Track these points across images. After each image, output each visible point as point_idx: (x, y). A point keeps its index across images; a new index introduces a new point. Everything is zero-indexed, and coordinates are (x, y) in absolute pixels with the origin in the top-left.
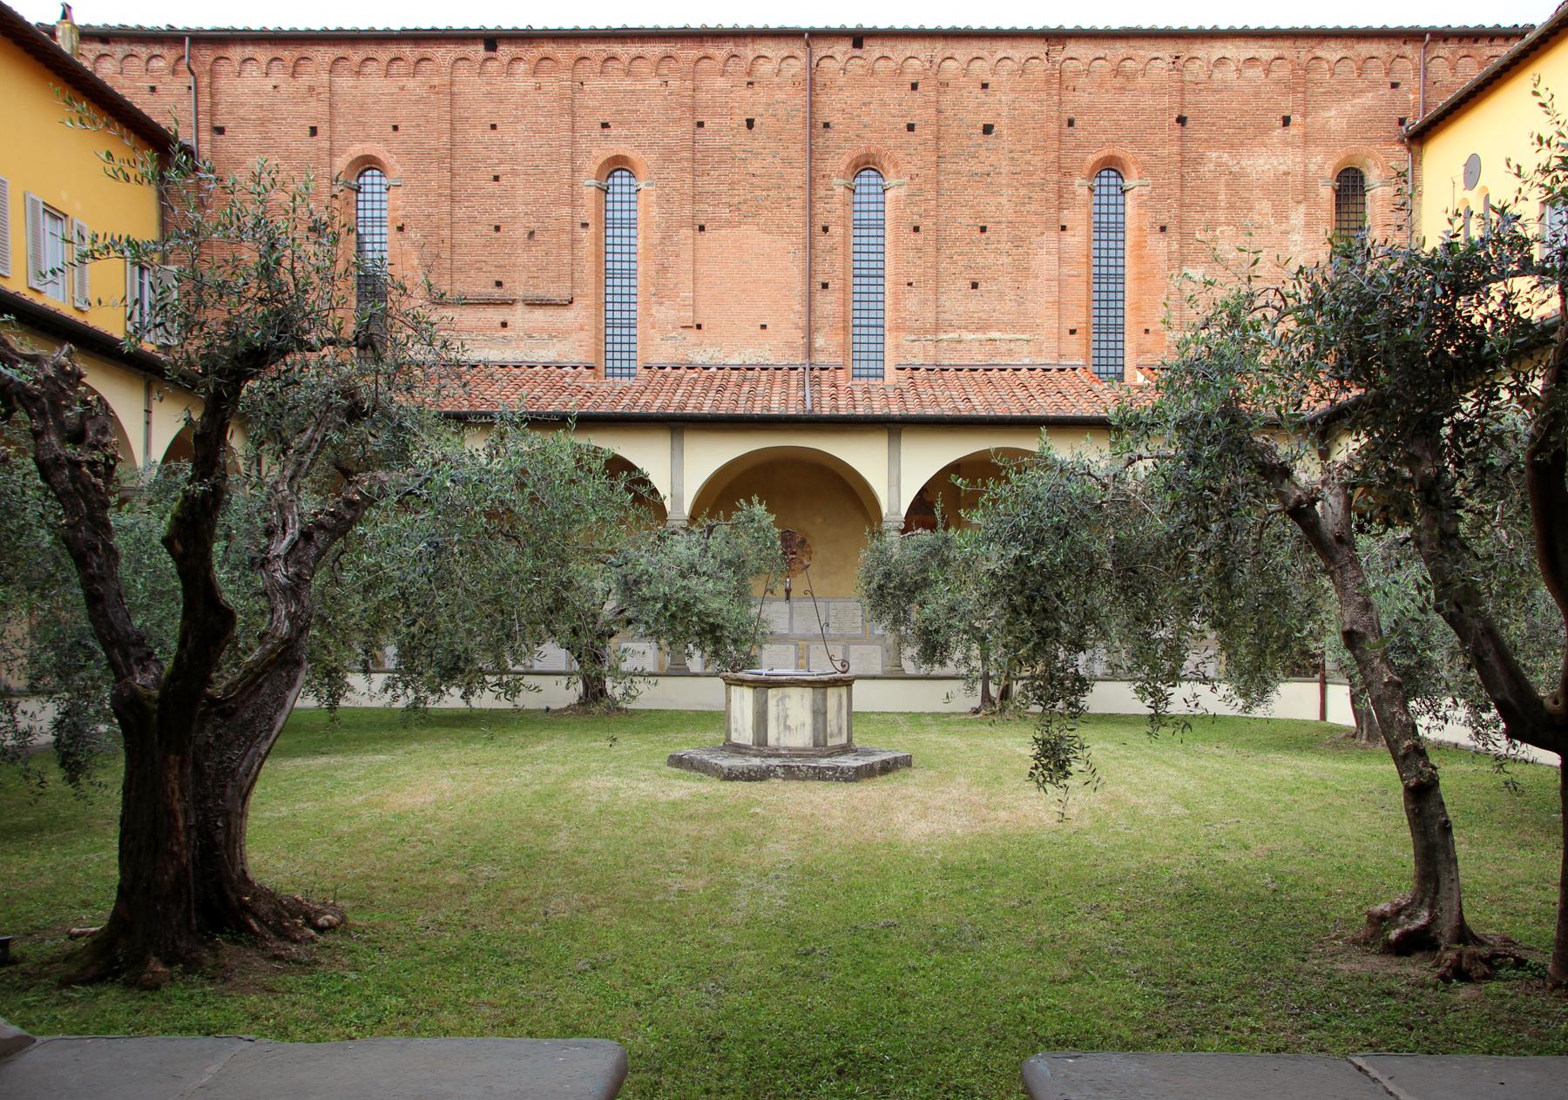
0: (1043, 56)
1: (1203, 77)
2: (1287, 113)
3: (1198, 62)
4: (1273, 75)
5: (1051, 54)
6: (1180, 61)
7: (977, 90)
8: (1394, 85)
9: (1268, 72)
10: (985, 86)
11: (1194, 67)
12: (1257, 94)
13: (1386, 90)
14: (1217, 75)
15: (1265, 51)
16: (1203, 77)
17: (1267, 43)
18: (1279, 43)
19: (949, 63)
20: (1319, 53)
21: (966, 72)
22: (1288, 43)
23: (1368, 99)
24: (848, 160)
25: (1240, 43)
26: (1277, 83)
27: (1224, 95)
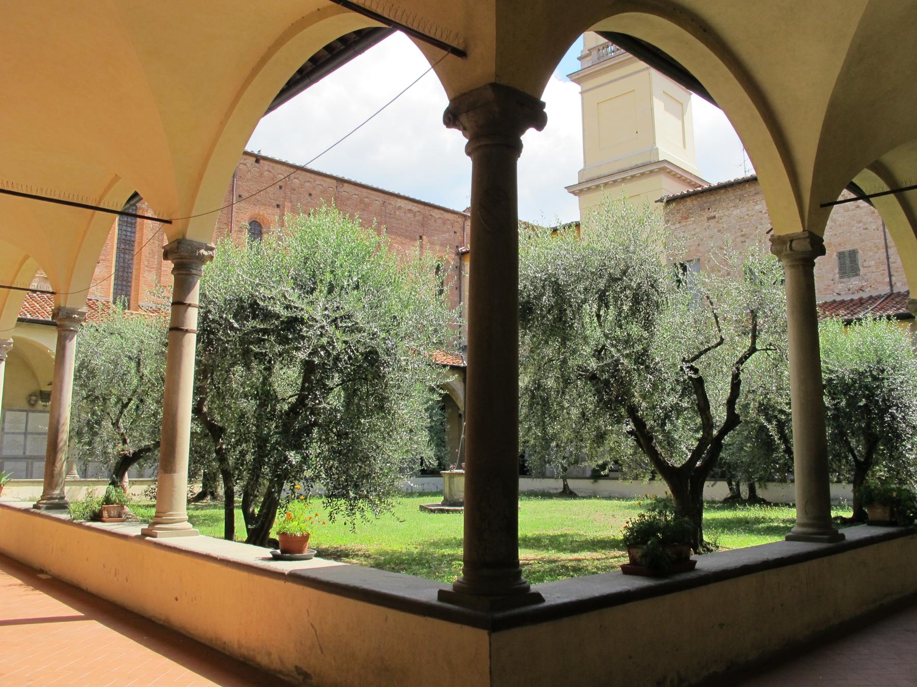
0: (335, 188)
1: (392, 212)
2: (421, 234)
3: (392, 206)
4: (417, 218)
5: (338, 188)
6: (386, 204)
7: (307, 196)
8: (455, 232)
9: (415, 216)
10: (310, 195)
11: (390, 207)
12: (411, 224)
13: (452, 233)
14: (398, 213)
15: (415, 208)
16: (392, 212)
17: (415, 204)
18: (419, 206)
19: (296, 180)
20: (433, 214)
21: (302, 186)
22: (422, 207)
23: (447, 235)
24: (248, 217)
25: (406, 202)
26: (418, 221)
27: (399, 222)
